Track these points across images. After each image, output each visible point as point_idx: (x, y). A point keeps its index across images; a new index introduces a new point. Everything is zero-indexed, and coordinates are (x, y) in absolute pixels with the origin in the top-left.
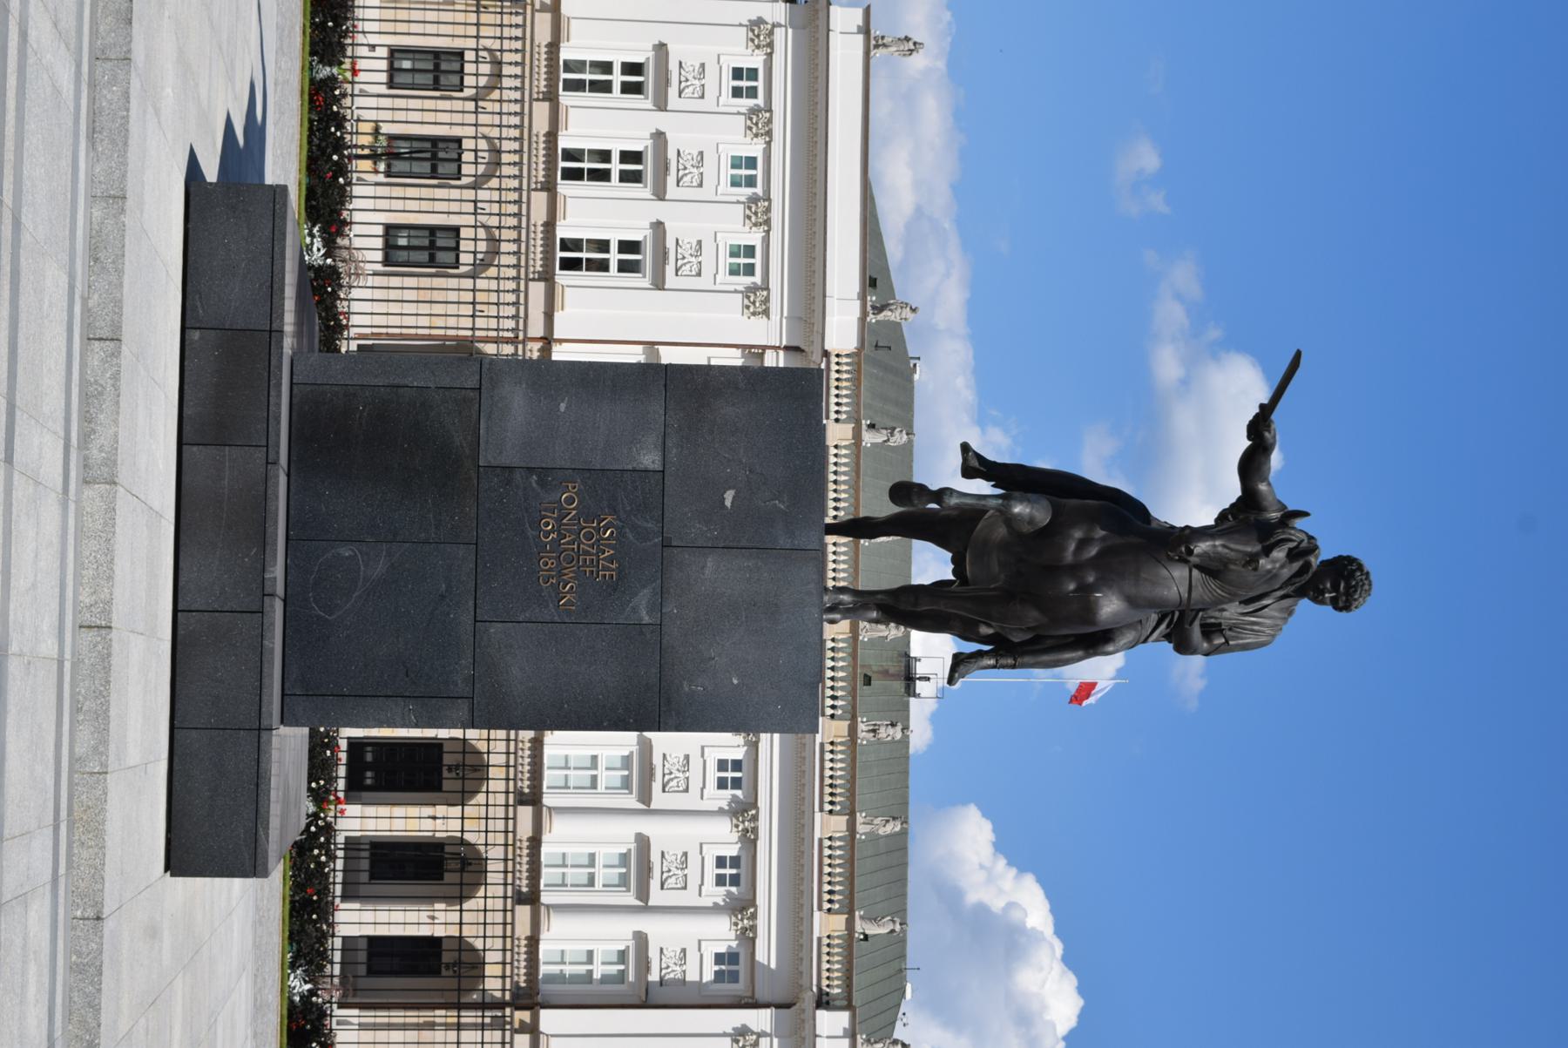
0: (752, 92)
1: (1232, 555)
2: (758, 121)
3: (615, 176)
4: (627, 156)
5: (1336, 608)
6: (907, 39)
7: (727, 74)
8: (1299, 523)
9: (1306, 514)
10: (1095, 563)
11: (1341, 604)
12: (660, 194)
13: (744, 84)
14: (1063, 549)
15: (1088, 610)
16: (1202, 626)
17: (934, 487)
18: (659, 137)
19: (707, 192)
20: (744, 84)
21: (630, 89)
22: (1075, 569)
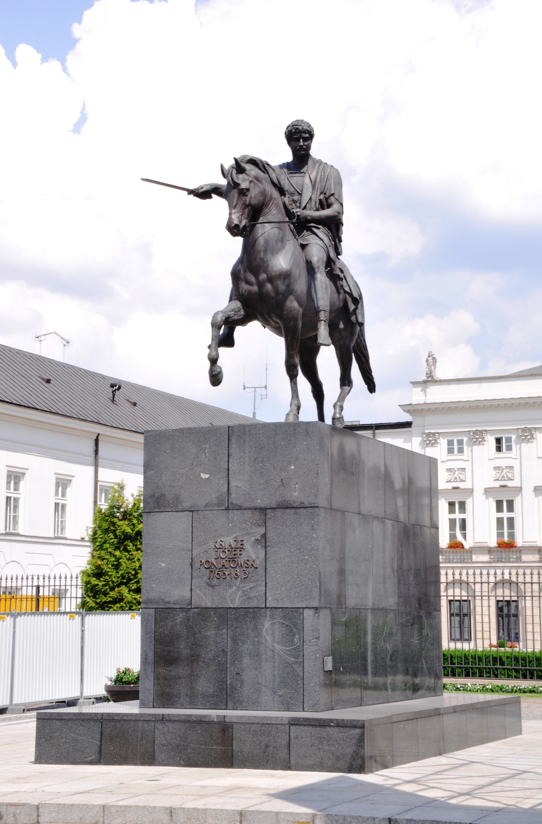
0: (460, 442)
1: (240, 203)
2: (477, 438)
3: (511, 515)
4: (499, 508)
5: (311, 136)
6: (427, 361)
7: (500, 455)
8: (227, 167)
9: (222, 167)
10: (256, 274)
11: (307, 135)
12: (519, 490)
13: (456, 447)
14: (250, 292)
15: (286, 276)
16: (323, 208)
17: (208, 364)
18: (488, 491)
19: (515, 463)
20: (456, 447)
21: (511, 506)
22: (261, 285)
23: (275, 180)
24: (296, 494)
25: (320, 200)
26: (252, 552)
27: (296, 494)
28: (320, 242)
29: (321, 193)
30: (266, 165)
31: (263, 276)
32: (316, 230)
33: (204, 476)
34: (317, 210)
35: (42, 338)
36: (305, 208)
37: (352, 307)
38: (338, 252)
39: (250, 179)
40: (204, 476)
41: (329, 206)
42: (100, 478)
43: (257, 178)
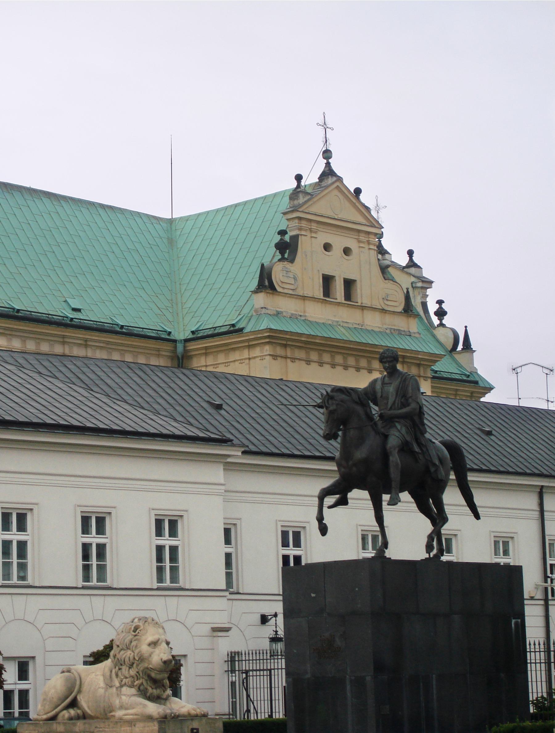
23: (357, 400)
24: (359, 606)
25: (401, 402)
26: (338, 642)
27: (359, 606)
28: (397, 434)
29: (402, 397)
30: (350, 391)
31: (350, 463)
32: (397, 424)
33: (313, 595)
34: (401, 408)
35: (519, 370)
36: (391, 408)
37: (432, 469)
38: (423, 432)
39: (337, 402)
40: (313, 595)
41: (408, 405)
42: (547, 533)
43: (342, 401)
